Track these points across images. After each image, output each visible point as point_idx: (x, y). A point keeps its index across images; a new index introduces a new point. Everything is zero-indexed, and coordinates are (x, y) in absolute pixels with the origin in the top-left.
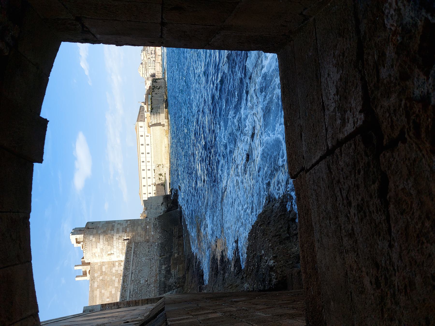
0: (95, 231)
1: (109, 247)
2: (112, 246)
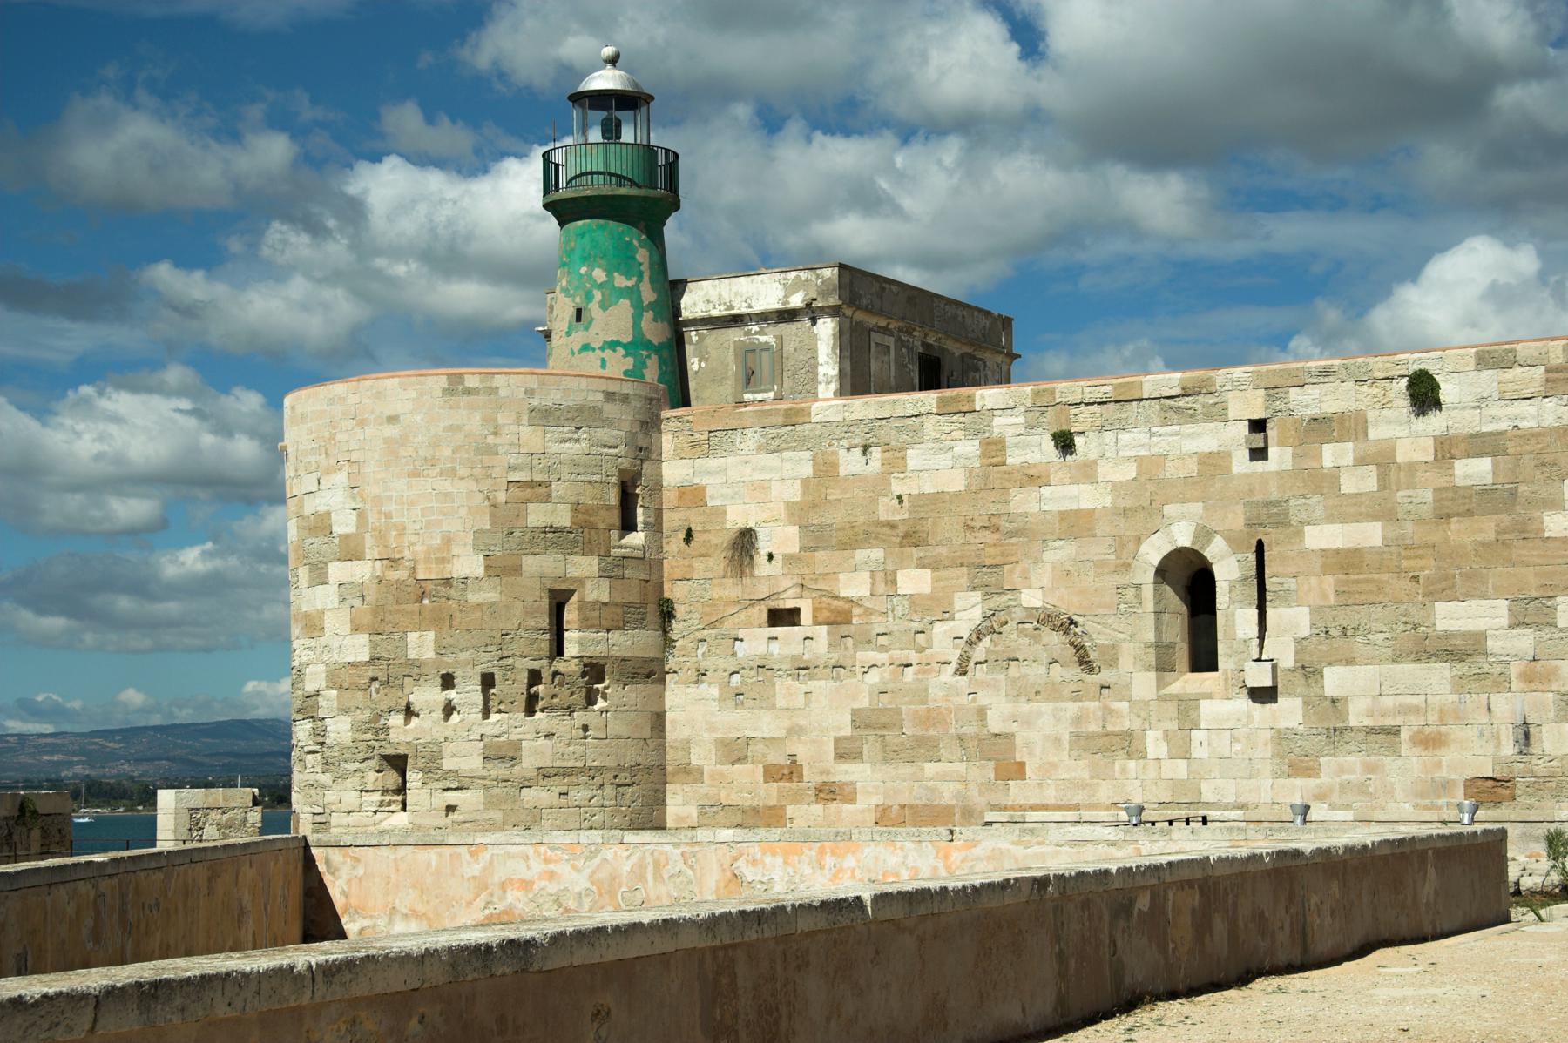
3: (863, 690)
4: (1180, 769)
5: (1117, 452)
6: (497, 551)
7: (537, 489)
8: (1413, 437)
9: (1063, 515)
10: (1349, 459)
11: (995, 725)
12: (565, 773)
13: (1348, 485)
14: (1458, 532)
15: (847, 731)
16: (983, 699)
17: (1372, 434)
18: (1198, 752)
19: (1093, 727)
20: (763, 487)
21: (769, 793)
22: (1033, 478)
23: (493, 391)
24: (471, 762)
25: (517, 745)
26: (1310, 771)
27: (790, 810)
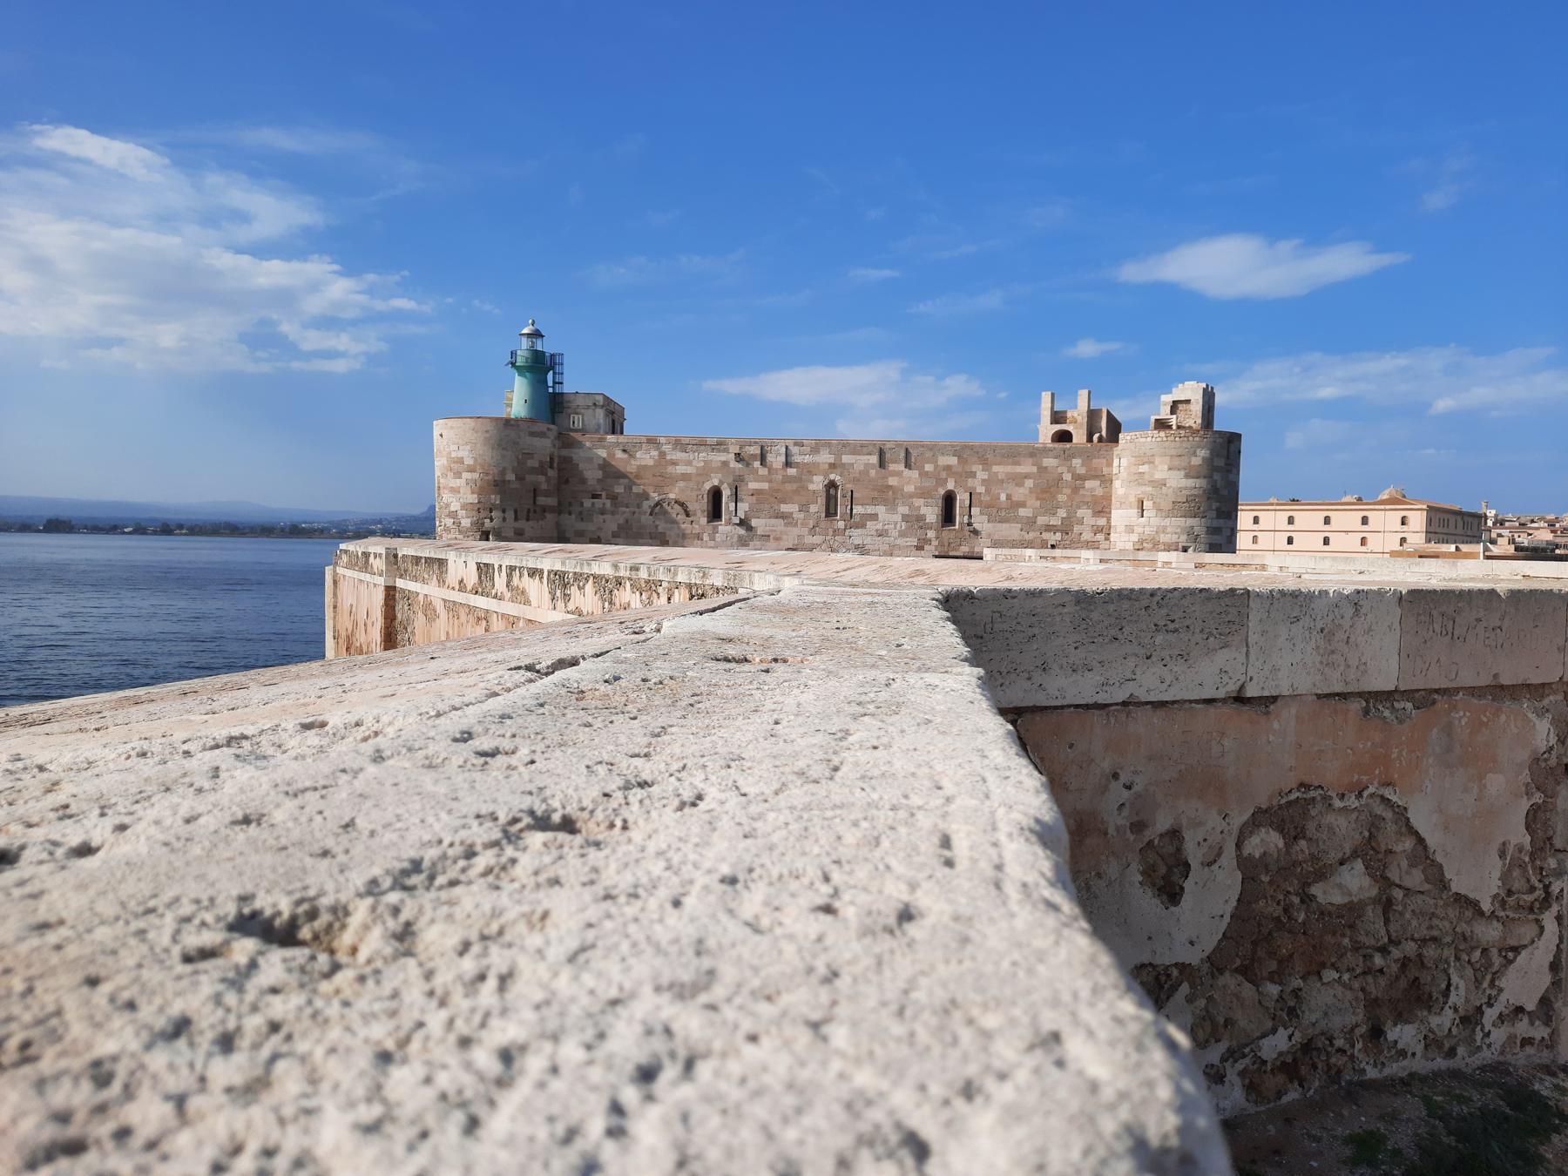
0: (1220, 462)
1: (1166, 505)
2: (1169, 514)
14: (788, 487)
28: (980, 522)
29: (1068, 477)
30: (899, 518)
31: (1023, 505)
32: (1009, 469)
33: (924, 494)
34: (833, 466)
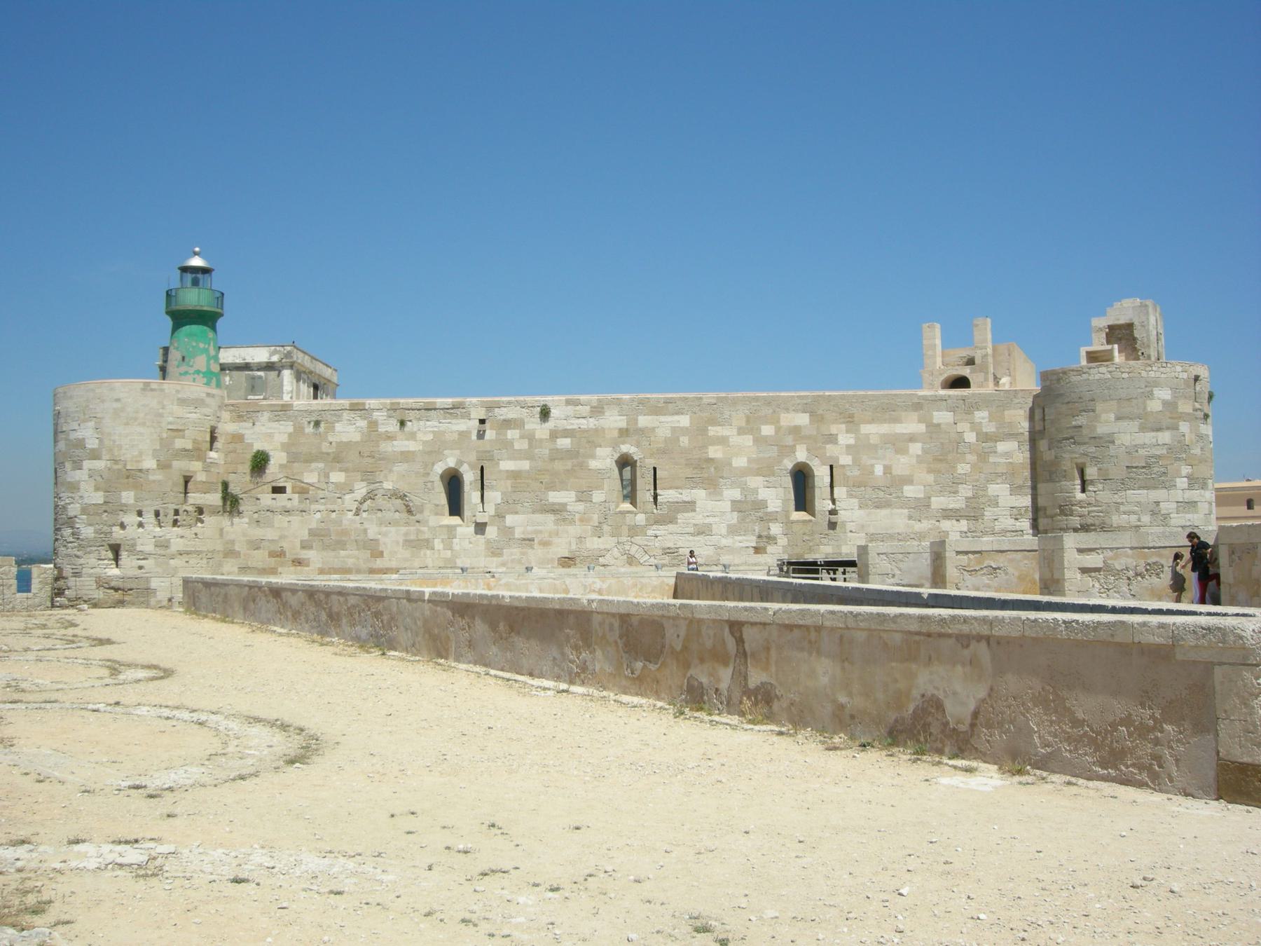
3: (314, 520)
4: (449, 553)
5: (424, 430)
6: (162, 458)
7: (179, 432)
8: (542, 431)
9: (402, 453)
10: (517, 436)
11: (371, 534)
12: (188, 553)
13: (517, 446)
14: (559, 466)
15: (306, 538)
16: (366, 525)
17: (526, 427)
18: (457, 547)
19: (412, 537)
20: (271, 435)
21: (272, 562)
22: (390, 437)
23: (162, 390)
24: (149, 548)
25: (168, 541)
26: (501, 555)
27: (280, 569)
28: (850, 511)
29: (970, 437)
30: (727, 506)
31: (909, 480)
32: (885, 428)
33: (764, 469)
34: (624, 433)
